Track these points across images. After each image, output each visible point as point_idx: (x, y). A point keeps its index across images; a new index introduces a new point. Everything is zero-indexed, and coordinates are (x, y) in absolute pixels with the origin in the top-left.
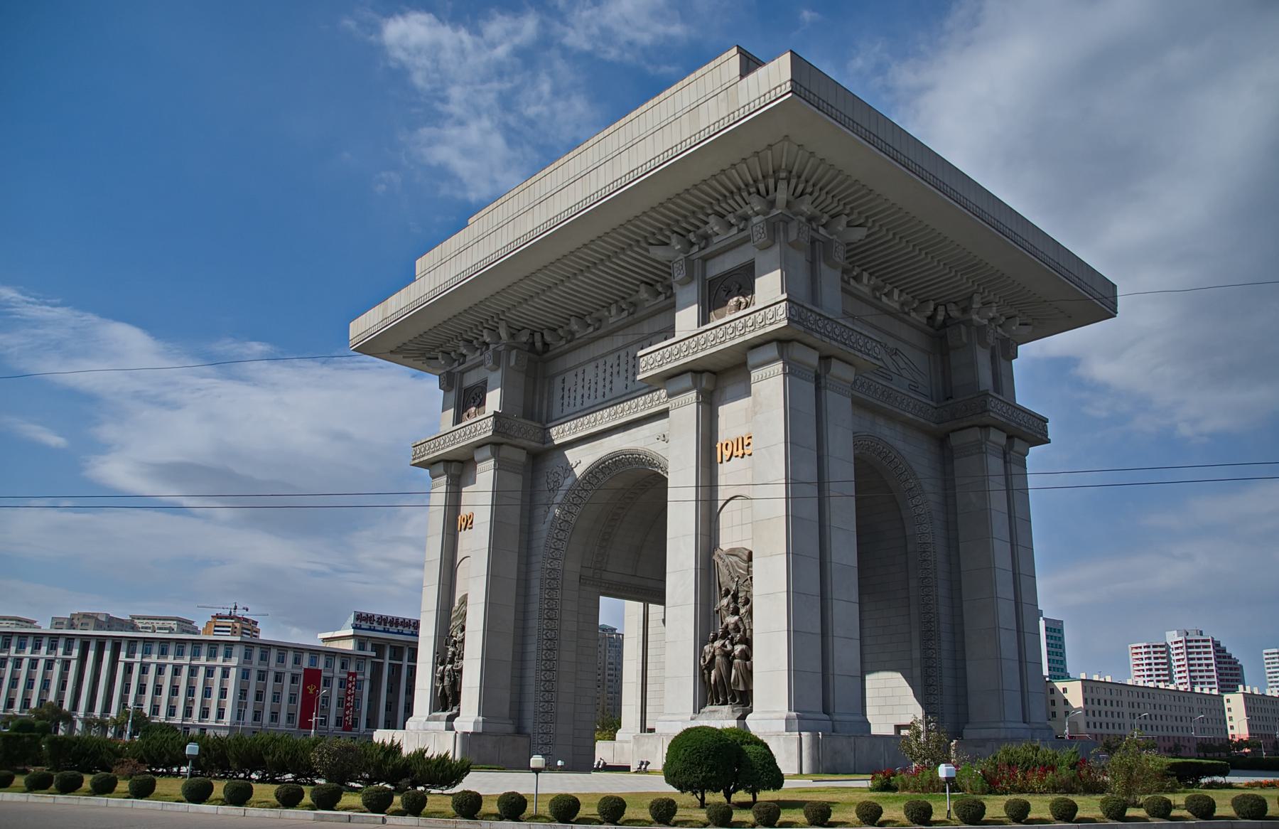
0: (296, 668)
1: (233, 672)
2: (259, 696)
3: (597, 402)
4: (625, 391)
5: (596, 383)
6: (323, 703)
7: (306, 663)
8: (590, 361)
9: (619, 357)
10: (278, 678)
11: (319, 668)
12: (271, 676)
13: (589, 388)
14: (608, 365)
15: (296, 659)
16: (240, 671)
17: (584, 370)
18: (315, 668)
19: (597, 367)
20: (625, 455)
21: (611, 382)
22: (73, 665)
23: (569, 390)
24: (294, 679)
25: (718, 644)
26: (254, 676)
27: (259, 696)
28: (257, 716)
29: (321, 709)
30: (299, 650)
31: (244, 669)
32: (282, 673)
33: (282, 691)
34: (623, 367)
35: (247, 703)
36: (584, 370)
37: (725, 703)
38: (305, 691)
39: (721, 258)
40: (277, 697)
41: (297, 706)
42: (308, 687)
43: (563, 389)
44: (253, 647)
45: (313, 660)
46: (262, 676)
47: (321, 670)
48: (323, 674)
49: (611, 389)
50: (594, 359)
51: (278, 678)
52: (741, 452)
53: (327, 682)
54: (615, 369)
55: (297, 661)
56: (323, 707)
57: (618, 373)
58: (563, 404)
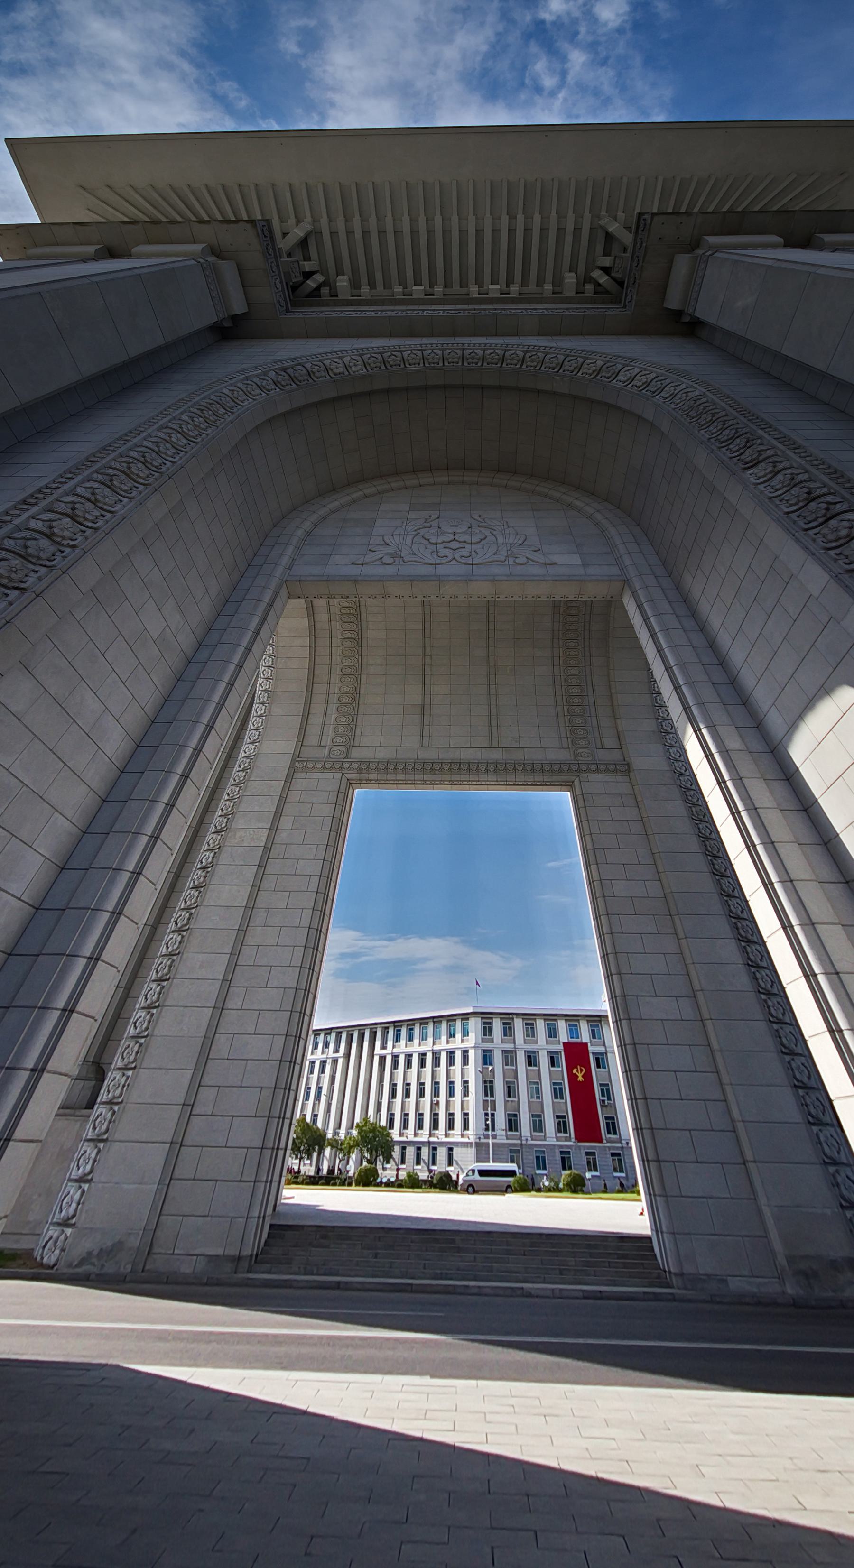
0: (552, 1043)
1: (472, 1054)
2: (511, 1091)
6: (603, 1095)
7: (563, 1035)
10: (531, 1059)
11: (584, 1041)
12: (521, 1058)
15: (549, 1030)
16: (480, 1052)
18: (578, 1040)
22: (340, 1061)
24: (553, 1062)
26: (498, 1057)
27: (511, 1091)
28: (513, 1123)
29: (602, 1106)
30: (551, 1018)
31: (484, 1051)
32: (534, 1052)
33: (540, 1079)
35: (494, 1101)
38: (572, 1078)
40: (536, 1090)
41: (566, 1102)
42: (575, 1071)
44: (492, 1018)
45: (573, 1030)
46: (509, 1057)
47: (586, 1044)
48: (591, 1049)
51: (531, 1059)
53: (601, 1061)
55: (552, 1033)
56: (603, 1101)
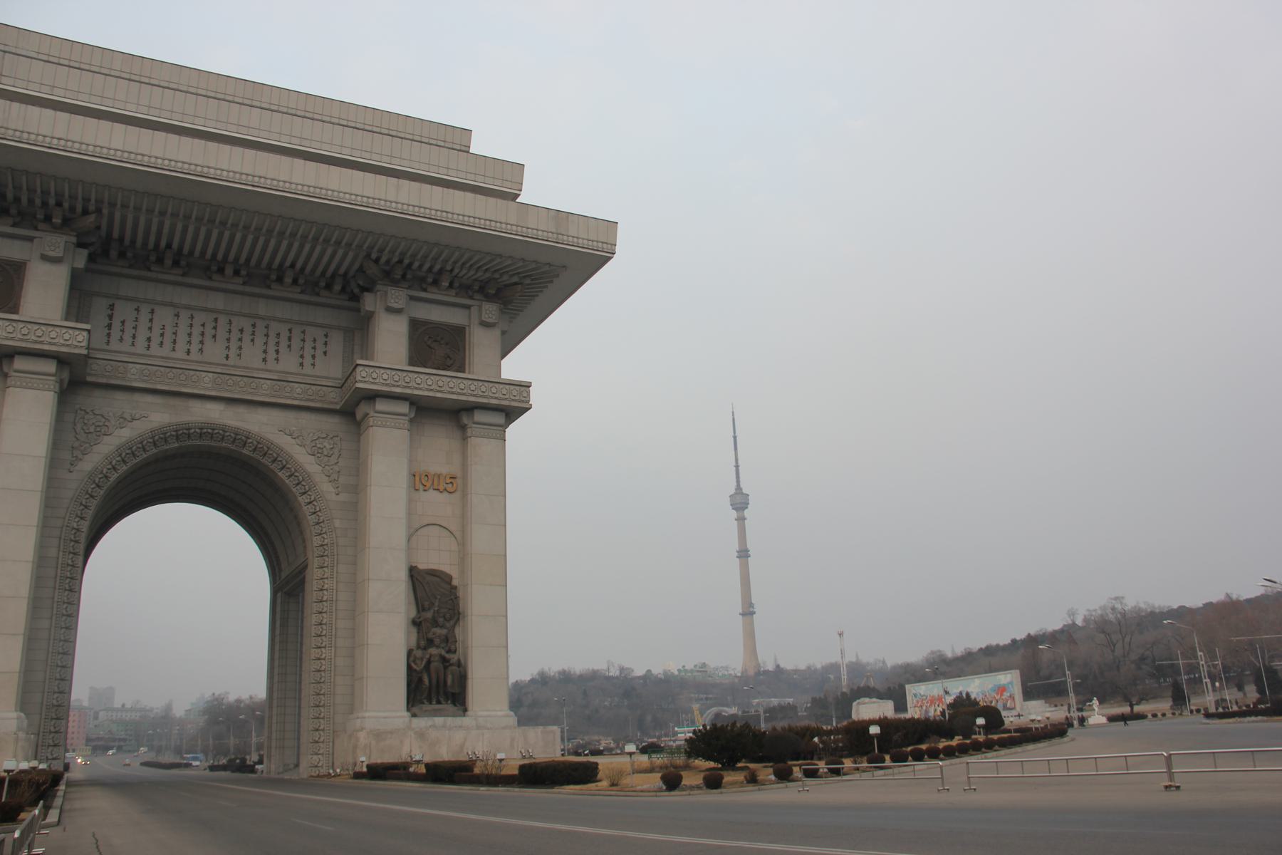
3: (173, 355)
4: (225, 362)
5: (175, 334)
8: (164, 304)
9: (216, 320)
13: (162, 335)
14: (197, 322)
17: (153, 310)
19: (177, 315)
20: (224, 431)
21: (202, 342)
23: (123, 322)
25: (433, 651)
34: (222, 333)
36: (153, 310)
37: (439, 702)
39: (427, 305)
43: (111, 317)
49: (201, 350)
50: (172, 305)
52: (442, 488)
54: (209, 331)
57: (214, 336)
58: (109, 335)
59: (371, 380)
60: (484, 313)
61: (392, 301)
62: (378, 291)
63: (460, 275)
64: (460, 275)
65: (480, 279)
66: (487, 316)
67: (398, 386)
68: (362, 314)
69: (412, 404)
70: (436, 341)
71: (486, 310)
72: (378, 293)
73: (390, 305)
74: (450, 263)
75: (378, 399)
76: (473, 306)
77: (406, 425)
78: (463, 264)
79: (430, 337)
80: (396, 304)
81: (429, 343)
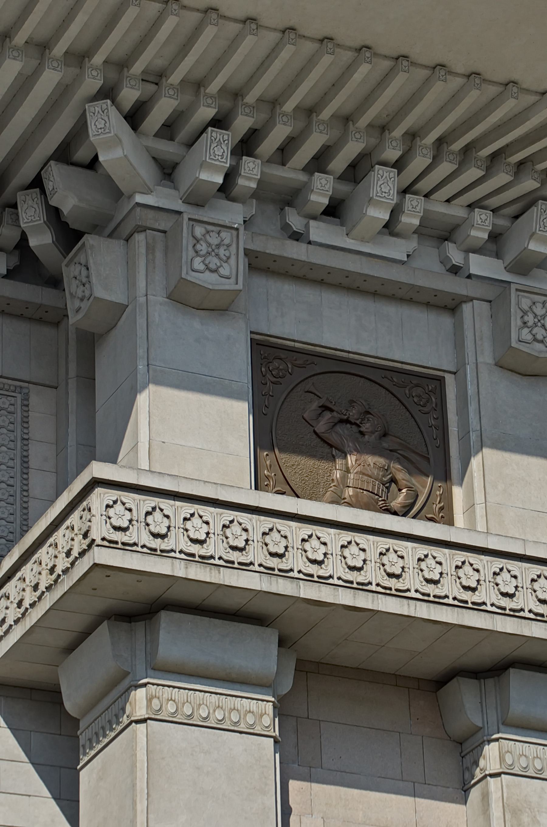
59: (146, 539)
60: (515, 322)
61: (198, 264)
62: (141, 229)
63: (425, 185)
64: (425, 185)
65: (496, 202)
66: (525, 334)
67: (245, 566)
68: (73, 319)
69: (281, 643)
70: (347, 421)
71: (525, 313)
72: (140, 238)
73: (193, 277)
74: (398, 132)
75: (164, 617)
76: (471, 299)
77: (267, 721)
78: (440, 142)
79: (325, 408)
80: (214, 276)
81: (321, 426)
